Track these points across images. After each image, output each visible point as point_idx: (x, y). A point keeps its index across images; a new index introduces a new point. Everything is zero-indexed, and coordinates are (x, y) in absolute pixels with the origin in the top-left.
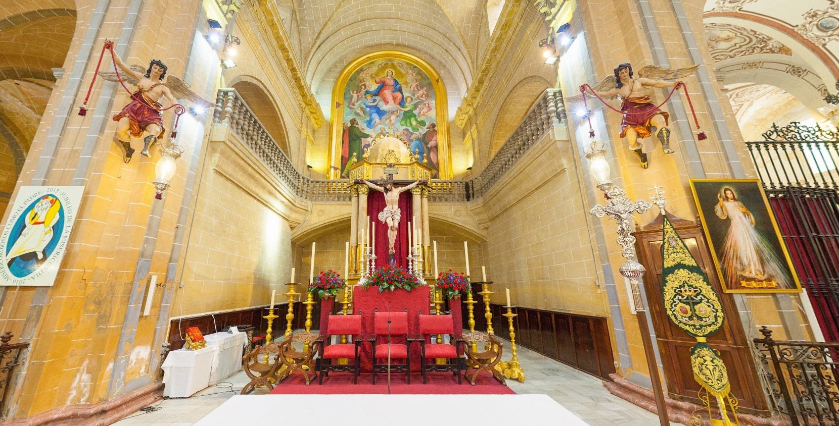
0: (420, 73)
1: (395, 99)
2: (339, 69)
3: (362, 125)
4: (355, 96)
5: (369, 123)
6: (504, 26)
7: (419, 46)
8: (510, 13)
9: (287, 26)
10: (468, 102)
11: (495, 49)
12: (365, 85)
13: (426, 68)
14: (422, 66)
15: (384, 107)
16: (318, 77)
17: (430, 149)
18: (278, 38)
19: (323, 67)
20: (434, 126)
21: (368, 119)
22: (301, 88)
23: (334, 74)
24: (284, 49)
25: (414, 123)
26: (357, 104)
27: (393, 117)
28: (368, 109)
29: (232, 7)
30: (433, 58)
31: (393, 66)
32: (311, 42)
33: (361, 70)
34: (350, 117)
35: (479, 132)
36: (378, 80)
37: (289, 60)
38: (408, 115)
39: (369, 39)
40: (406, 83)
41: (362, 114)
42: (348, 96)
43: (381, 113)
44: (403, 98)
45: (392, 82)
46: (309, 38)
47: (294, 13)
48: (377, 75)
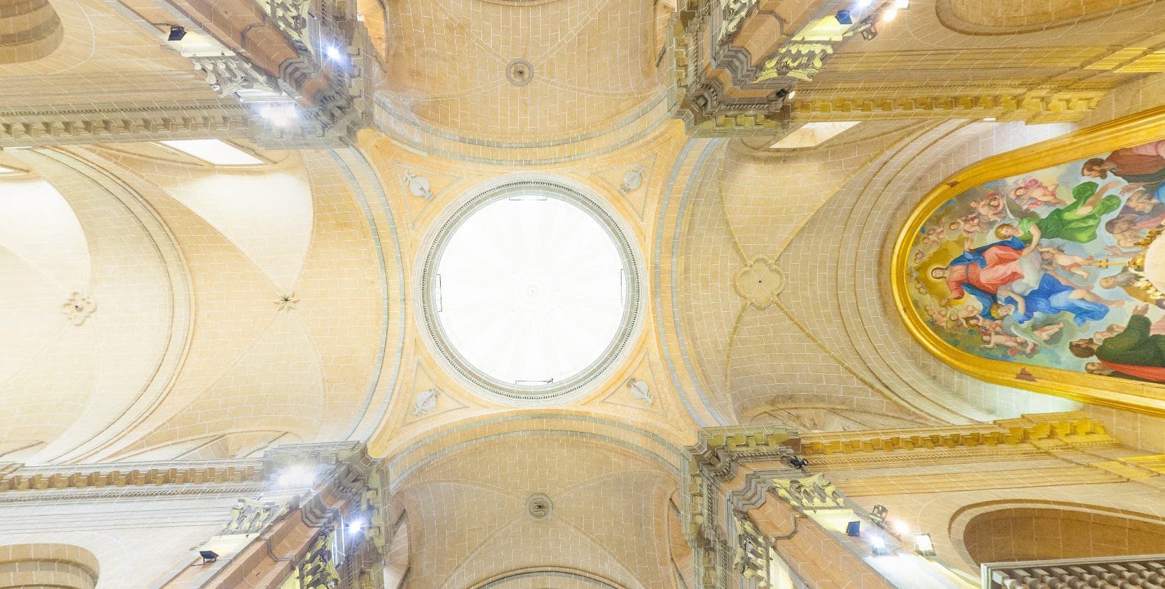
0: (936, 220)
1: (1002, 261)
2: (932, 362)
4: (995, 339)
6: (843, 107)
7: (882, 230)
8: (824, 109)
9: (853, 427)
10: (1008, 108)
11: (884, 105)
12: (967, 319)
13: (926, 211)
14: (920, 218)
15: (1030, 279)
16: (950, 402)
18: (873, 446)
19: (926, 387)
20: (1094, 164)
21: (1070, 316)
22: (977, 440)
23: (943, 372)
24: (893, 444)
25: (1083, 211)
26: (1022, 337)
28: (1037, 314)
29: (829, 490)
30: (903, 203)
31: (922, 268)
32: (878, 398)
33: (933, 323)
34: (1067, 356)
35: (1113, 49)
36: (955, 294)
37: (914, 443)
38: (1056, 227)
39: (871, 307)
41: (1053, 329)
42: (999, 354)
43: (1049, 287)
44: (1002, 244)
45: (959, 271)
46: (873, 400)
47: (833, 411)
48: (941, 296)
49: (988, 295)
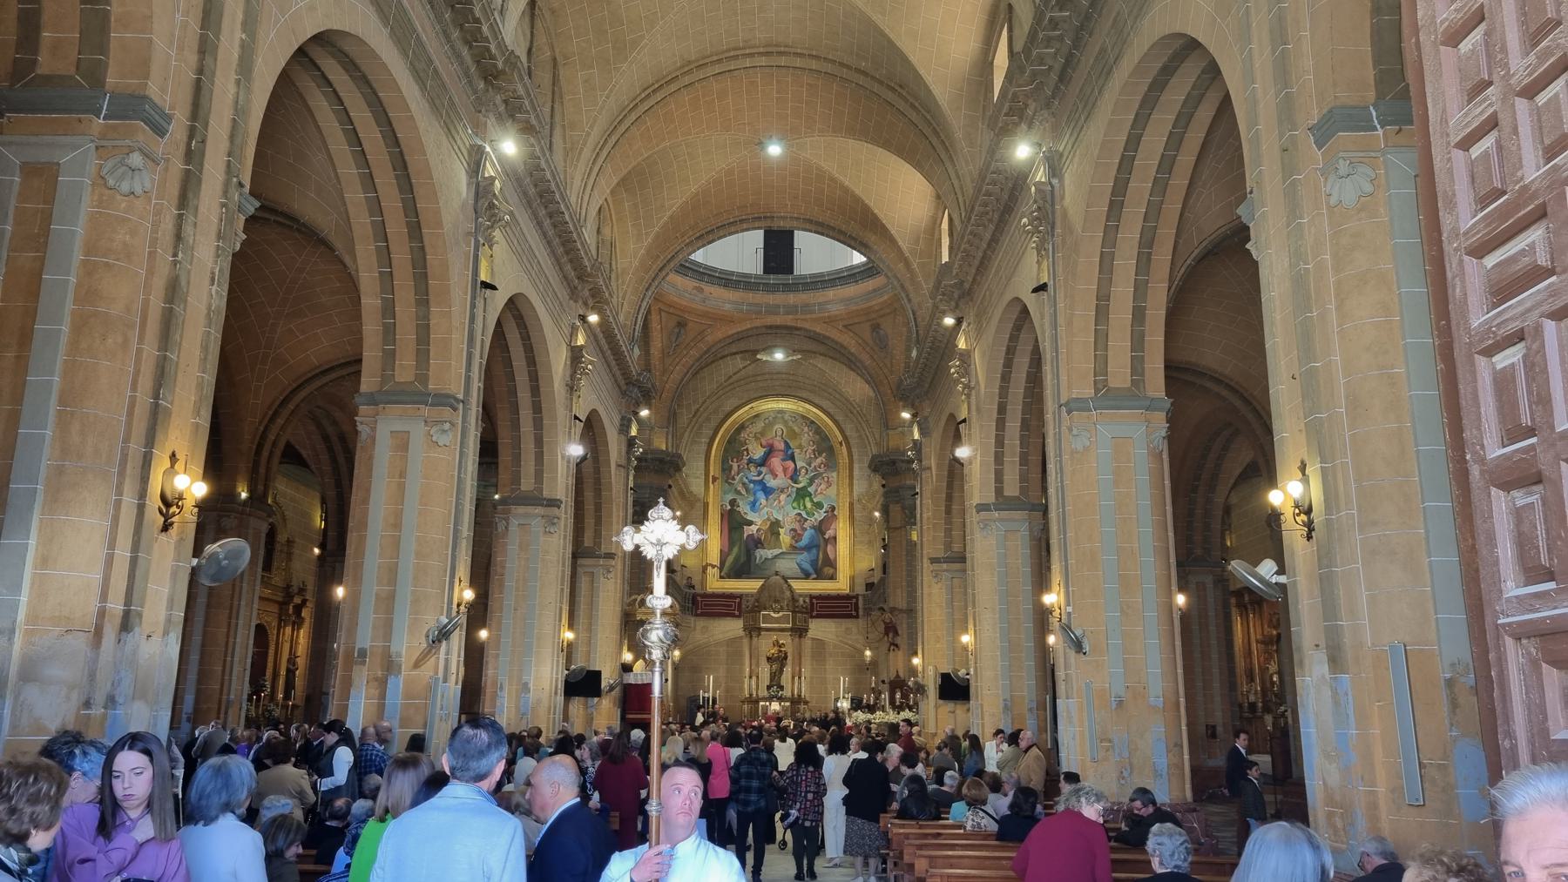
1: (785, 470)
3: (744, 508)
4: (735, 466)
5: (753, 505)
15: (772, 483)
17: (826, 541)
20: (833, 508)
25: (809, 505)
27: (783, 497)
33: (742, 427)
34: (730, 497)
38: (802, 494)
40: (800, 447)
43: (768, 491)
45: (782, 446)
49: (763, 462)
